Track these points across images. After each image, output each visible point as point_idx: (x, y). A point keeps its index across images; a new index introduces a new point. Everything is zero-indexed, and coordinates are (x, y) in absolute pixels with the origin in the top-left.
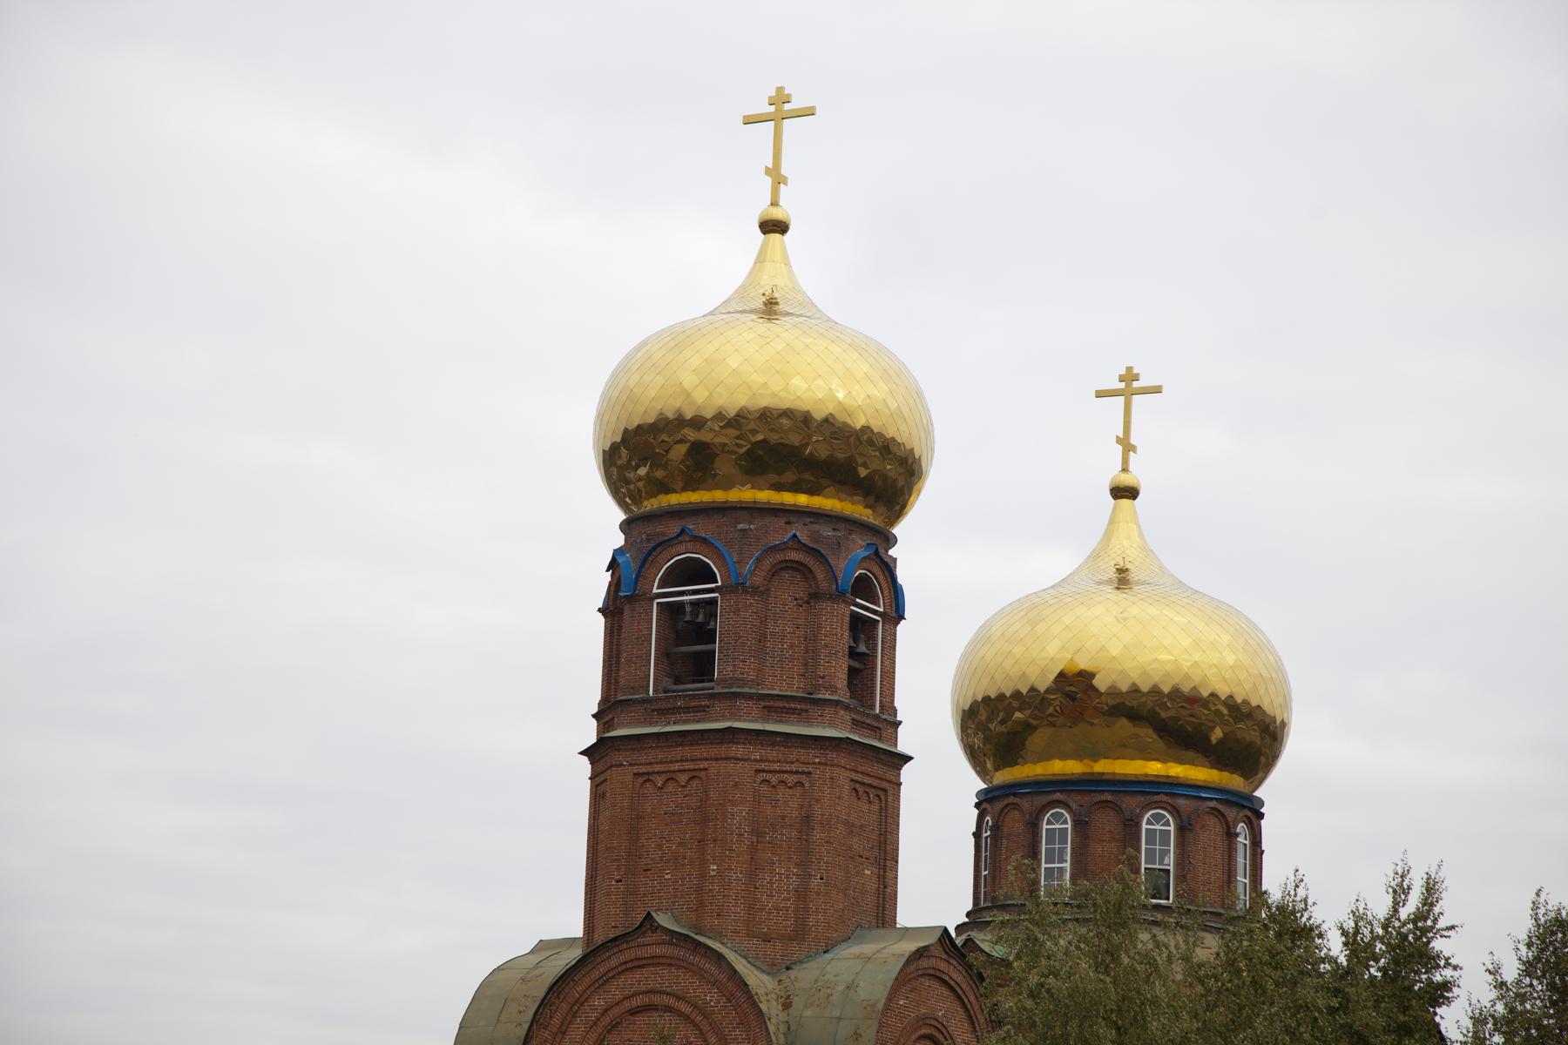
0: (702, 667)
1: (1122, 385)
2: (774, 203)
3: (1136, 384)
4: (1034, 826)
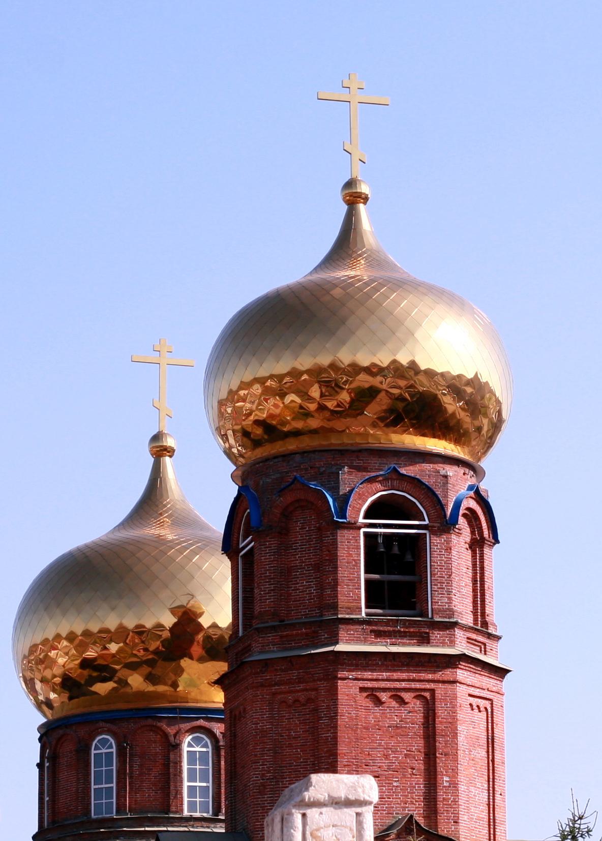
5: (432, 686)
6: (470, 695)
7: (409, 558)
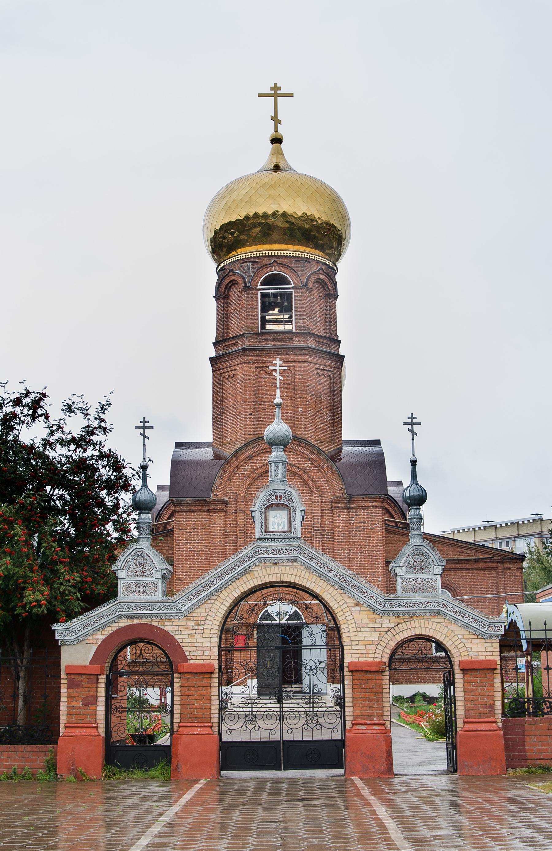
2: (276, 131)
5: (293, 364)
7: (286, 304)
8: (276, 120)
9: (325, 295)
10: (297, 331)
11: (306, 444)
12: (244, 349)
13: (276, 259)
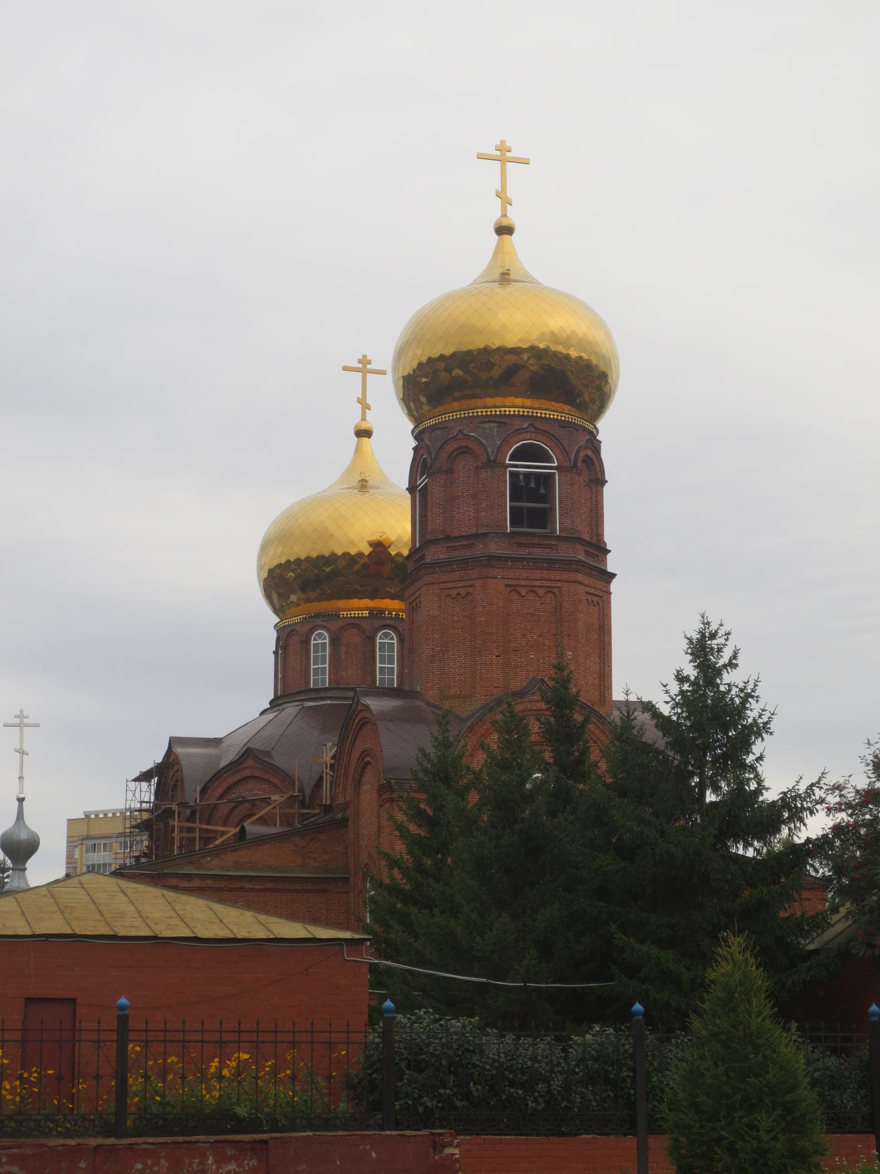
0: (542, 518)
1: (360, 366)
2: (504, 215)
3: (369, 366)
4: (307, 642)
5: (559, 584)
6: (587, 593)
8: (503, 197)
9: (591, 481)
10: (564, 535)
11: (582, 707)
12: (490, 557)
13: (535, 424)
